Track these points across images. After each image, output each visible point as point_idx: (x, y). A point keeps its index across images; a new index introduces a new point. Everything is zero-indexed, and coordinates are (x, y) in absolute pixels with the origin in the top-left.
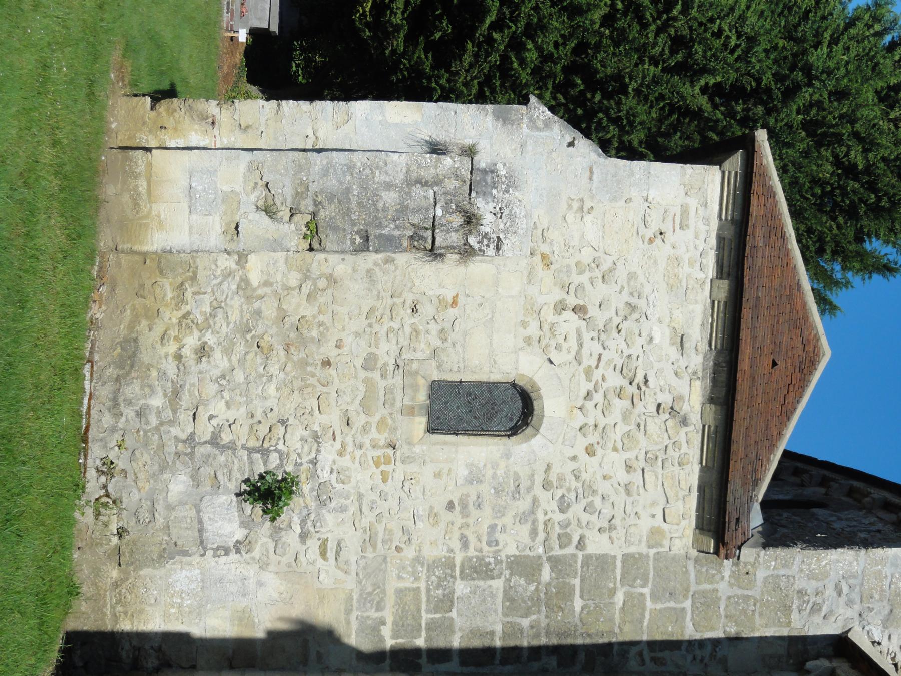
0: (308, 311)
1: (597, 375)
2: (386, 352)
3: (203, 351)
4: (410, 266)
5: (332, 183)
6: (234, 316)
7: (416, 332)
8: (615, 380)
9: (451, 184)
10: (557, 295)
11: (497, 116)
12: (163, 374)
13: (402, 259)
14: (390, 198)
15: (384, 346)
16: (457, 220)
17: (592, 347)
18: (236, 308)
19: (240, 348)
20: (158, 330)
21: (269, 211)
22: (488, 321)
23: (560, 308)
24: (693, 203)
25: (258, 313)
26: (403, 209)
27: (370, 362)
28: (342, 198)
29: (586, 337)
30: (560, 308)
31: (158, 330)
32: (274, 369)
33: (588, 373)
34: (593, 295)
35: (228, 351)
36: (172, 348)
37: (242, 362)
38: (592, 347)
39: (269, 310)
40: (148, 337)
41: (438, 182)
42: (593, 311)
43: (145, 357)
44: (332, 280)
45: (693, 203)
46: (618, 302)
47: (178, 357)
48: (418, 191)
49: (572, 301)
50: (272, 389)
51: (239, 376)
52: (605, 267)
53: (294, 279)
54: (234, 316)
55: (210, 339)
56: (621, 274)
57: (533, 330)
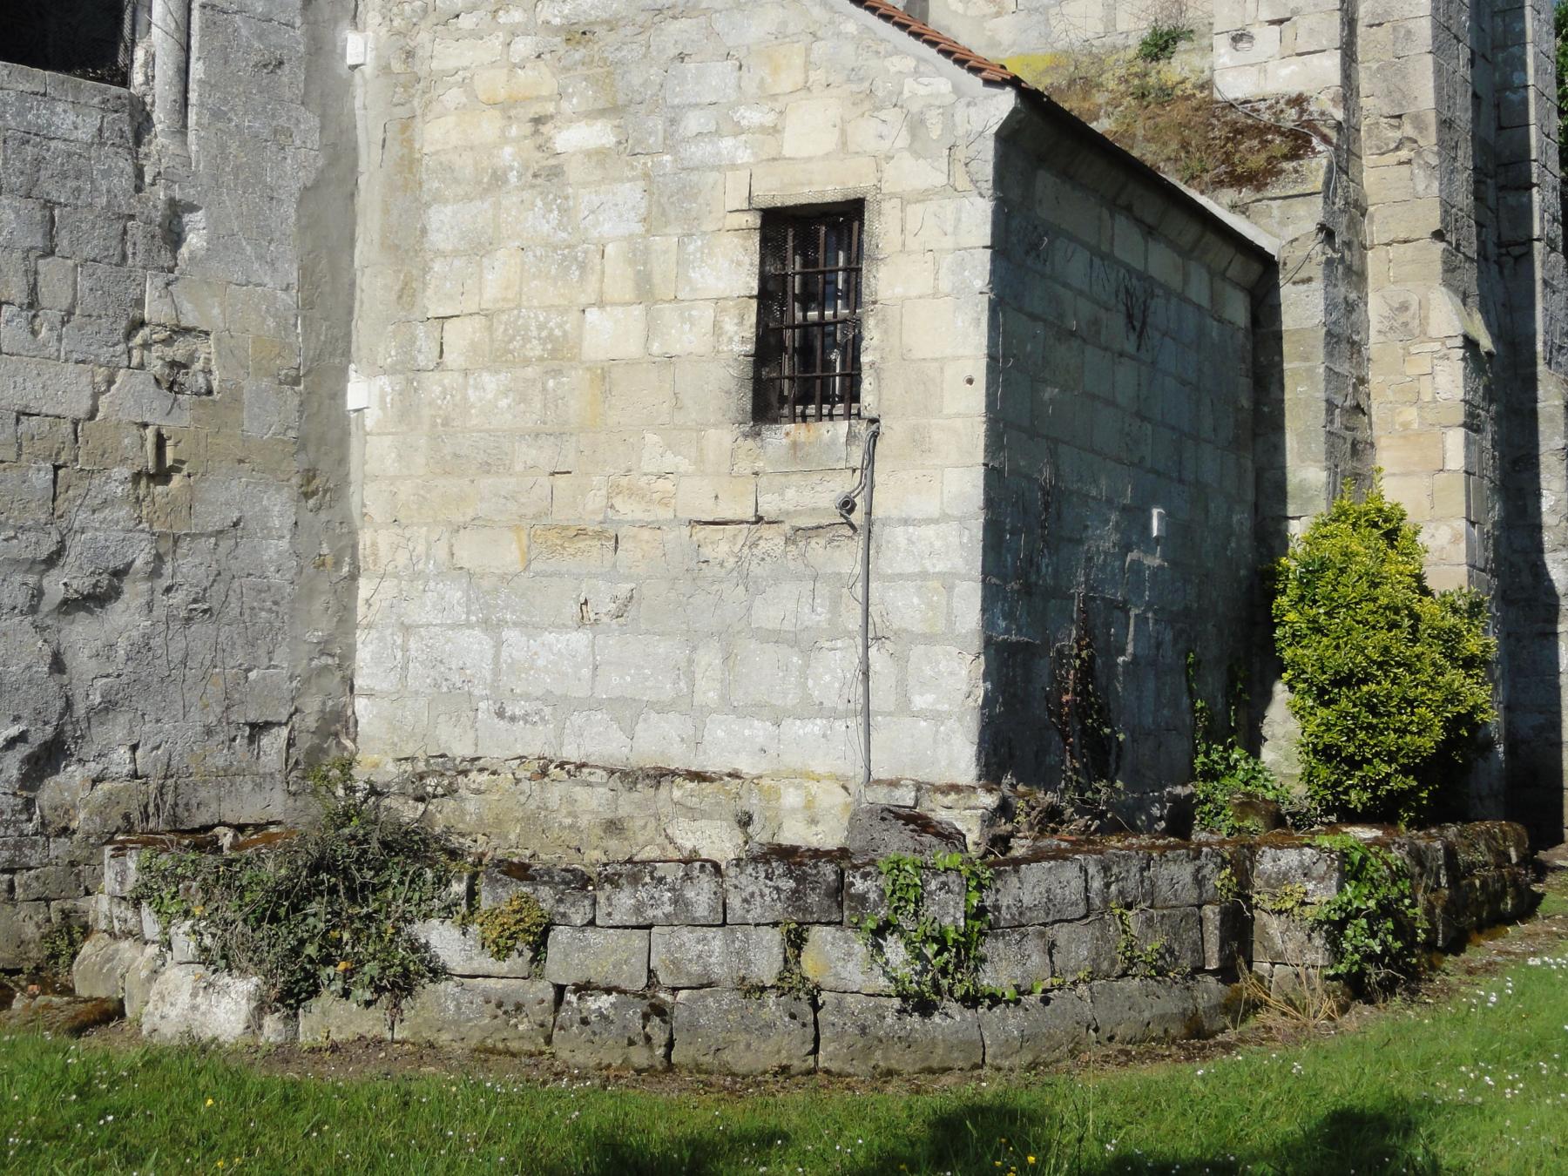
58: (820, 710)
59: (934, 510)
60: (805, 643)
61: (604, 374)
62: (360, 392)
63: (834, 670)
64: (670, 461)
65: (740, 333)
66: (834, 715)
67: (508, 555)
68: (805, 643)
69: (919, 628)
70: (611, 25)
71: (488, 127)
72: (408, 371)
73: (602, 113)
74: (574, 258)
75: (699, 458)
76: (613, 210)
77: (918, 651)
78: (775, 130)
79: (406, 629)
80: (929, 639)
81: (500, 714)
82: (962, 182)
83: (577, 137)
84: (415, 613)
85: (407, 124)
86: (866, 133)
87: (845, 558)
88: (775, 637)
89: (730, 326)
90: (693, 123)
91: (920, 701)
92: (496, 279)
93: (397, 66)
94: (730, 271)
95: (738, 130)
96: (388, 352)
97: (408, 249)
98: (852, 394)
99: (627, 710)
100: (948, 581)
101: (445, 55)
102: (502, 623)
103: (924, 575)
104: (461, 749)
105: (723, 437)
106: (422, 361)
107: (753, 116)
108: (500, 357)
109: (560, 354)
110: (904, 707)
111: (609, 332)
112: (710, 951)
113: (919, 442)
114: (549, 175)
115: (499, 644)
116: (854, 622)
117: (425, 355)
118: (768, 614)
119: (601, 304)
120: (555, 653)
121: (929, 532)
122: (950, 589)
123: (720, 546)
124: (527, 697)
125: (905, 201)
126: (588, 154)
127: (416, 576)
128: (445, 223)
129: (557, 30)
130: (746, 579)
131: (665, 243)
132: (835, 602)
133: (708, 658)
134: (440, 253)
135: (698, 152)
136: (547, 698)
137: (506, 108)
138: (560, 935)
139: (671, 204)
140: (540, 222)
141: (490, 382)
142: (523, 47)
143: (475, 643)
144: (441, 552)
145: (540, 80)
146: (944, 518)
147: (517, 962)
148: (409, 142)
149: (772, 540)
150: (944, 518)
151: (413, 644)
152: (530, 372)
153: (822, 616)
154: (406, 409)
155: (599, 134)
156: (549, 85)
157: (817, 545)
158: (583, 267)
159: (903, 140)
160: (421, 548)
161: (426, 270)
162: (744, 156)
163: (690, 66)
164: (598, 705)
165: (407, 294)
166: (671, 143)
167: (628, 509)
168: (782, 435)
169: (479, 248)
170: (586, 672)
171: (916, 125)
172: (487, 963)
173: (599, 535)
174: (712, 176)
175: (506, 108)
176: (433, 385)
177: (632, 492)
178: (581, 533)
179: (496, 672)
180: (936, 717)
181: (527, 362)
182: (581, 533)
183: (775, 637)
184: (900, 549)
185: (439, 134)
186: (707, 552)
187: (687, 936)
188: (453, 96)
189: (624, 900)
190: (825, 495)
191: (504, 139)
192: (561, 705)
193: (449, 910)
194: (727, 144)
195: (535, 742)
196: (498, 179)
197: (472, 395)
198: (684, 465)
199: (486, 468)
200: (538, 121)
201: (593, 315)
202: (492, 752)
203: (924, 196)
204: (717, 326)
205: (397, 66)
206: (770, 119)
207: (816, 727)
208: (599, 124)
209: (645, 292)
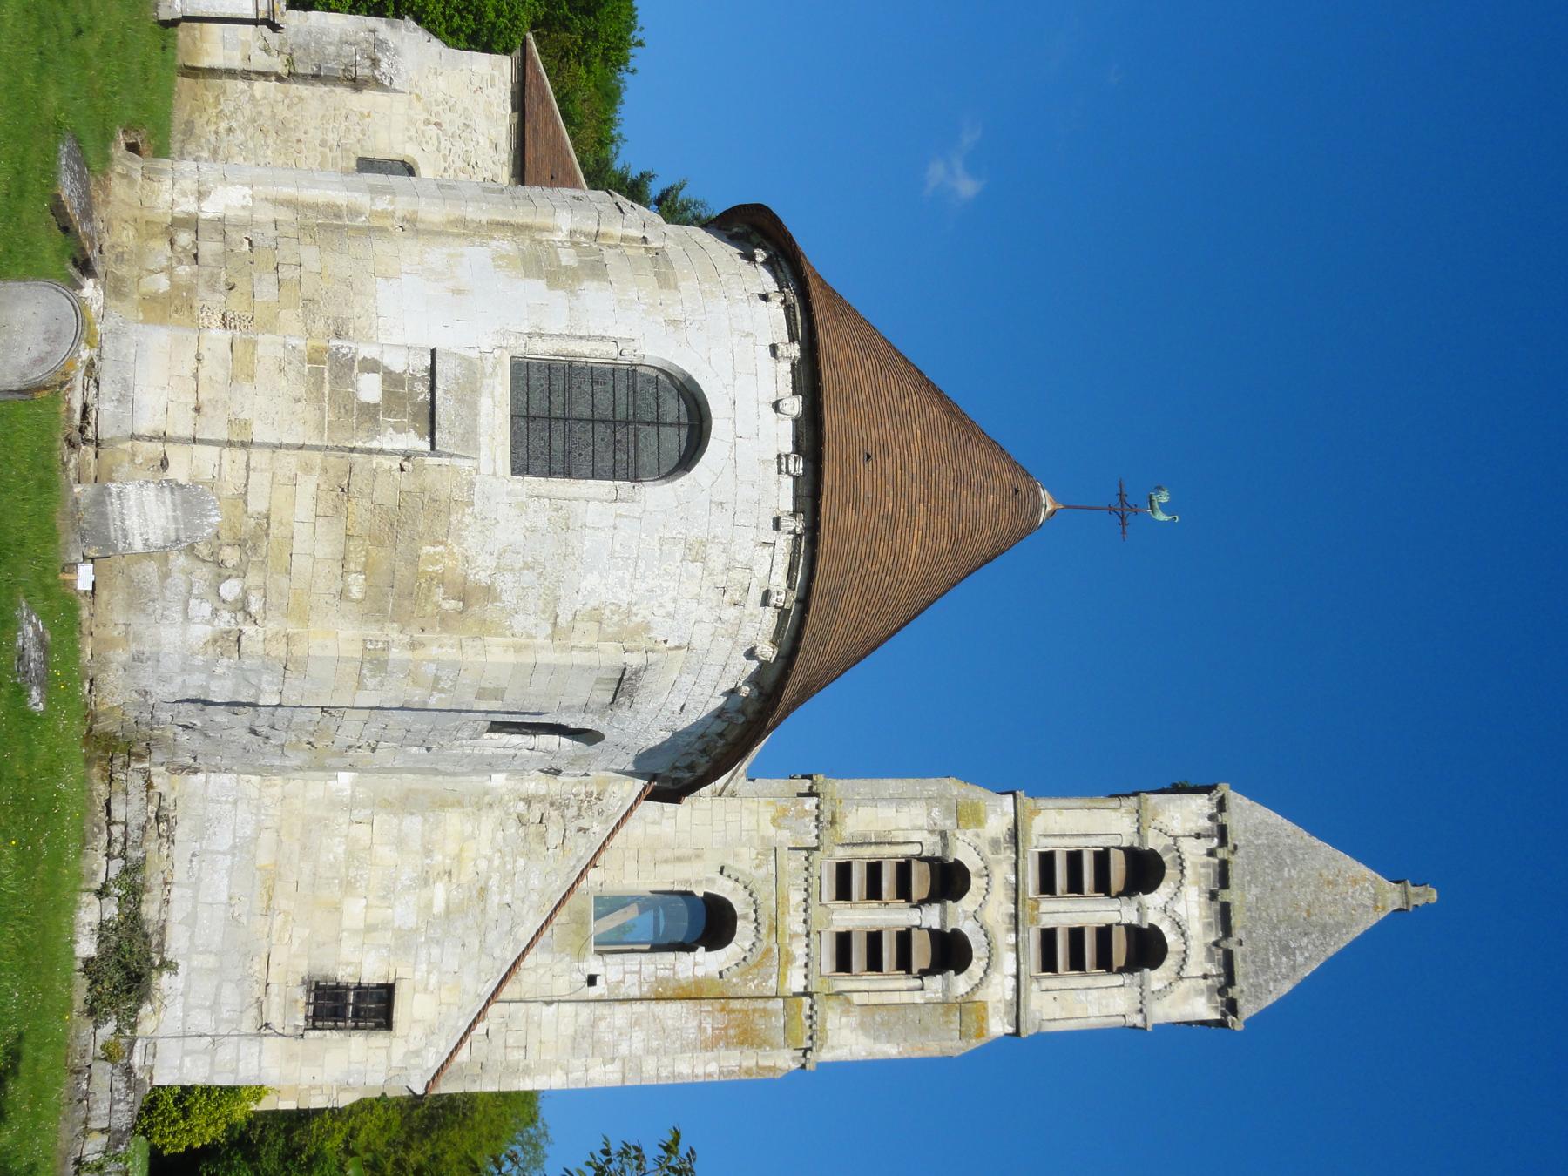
0: (288, 114)
1: (450, 159)
2: (332, 138)
3: (230, 130)
4: (342, 93)
5: (300, 40)
6: (247, 113)
7: (348, 129)
8: (460, 164)
9: (364, 45)
10: (425, 116)
11: (388, 24)
12: (208, 141)
13: (339, 90)
14: (331, 49)
15: (331, 136)
16: (368, 63)
17: (445, 145)
18: (248, 110)
19: (251, 130)
20: (205, 118)
21: (266, 50)
22: (385, 122)
23: (427, 122)
24: (497, 74)
25: (260, 113)
26: (339, 55)
27: (323, 143)
28: (306, 47)
29: (442, 139)
30: (427, 122)
31: (205, 118)
32: (270, 141)
33: (445, 158)
34: (446, 118)
35: (244, 131)
36: (213, 128)
37: (252, 137)
38: (445, 145)
39: (267, 112)
40: (200, 122)
41: (356, 43)
42: (445, 126)
43: (197, 131)
44: (301, 98)
45: (497, 74)
46: (459, 122)
47: (216, 133)
48: (346, 47)
49: (433, 120)
50: (269, 152)
51: (251, 145)
52: (451, 102)
53: (280, 97)
54: (247, 113)
55: (234, 124)
56: (459, 107)
57: (413, 133)
58: (186, 1015)
59: (264, 1064)
60: (214, 1008)
61: (337, 908)
62: (345, 778)
63: (202, 1021)
64: (296, 942)
65: (345, 975)
66: (184, 1022)
67: (264, 859)
68: (214, 1008)
69: (217, 1058)
70: (483, 911)
71: (452, 848)
72: (351, 805)
73: (448, 907)
74: (388, 893)
75: (297, 956)
76: (404, 913)
77: (208, 1058)
78: (426, 989)
79: (235, 803)
80: (212, 1063)
81: (193, 855)
82: (392, 1073)
83: (439, 894)
84: (242, 807)
85: (460, 804)
86: (418, 1031)
87: (248, 1026)
88: (218, 994)
89: (349, 970)
90: (435, 951)
91: (187, 1060)
92: (385, 853)
93: (487, 798)
94: (372, 975)
95: (429, 972)
96: (361, 794)
97: (406, 804)
98: (314, 1028)
99: (191, 921)
100: (235, 1071)
101: (489, 821)
102: (234, 855)
103: (238, 1061)
104: (179, 834)
105: (303, 968)
106: (355, 812)
107: (433, 979)
108: (351, 855)
109: (348, 886)
110: (186, 1053)
111: (355, 911)
112: (101, 1109)
113: (292, 1057)
114: (425, 880)
115: (224, 853)
116: (222, 1031)
117: (359, 814)
118: (228, 991)
119: (367, 907)
120: (218, 885)
121: (255, 1062)
122: (232, 1072)
123: (258, 966)
124: (200, 869)
125: (388, 1048)
126: (431, 900)
127: (258, 808)
128: (413, 825)
129: (486, 883)
130: (244, 978)
131: (388, 938)
132: (230, 1021)
133: (211, 961)
134: (401, 822)
135: (423, 954)
136: (199, 879)
137: (458, 858)
138: (109, 1066)
139: (405, 942)
140: (407, 875)
141: (340, 850)
142: (483, 865)
143: (224, 841)
144: (268, 823)
145: (466, 875)
146: (260, 1069)
147: (100, 1053)
148: (452, 805)
149: (258, 991)
150: (260, 1069)
151: (228, 806)
152: (343, 870)
153: (225, 1015)
154: (334, 804)
155: (439, 907)
156: (464, 880)
157: (254, 1012)
158: (384, 897)
159: (412, 1048)
160: (271, 812)
161: (395, 815)
162: (418, 975)
163: (459, 950)
164: (195, 907)
165: (386, 805)
166: (431, 941)
167: (278, 921)
168: (301, 995)
169: (400, 843)
170: (209, 900)
171: (417, 1053)
172: (100, 1043)
173: (268, 907)
174: (412, 961)
175: (458, 858)
176: (343, 819)
177: (285, 922)
178: (270, 898)
179: (212, 852)
180: (180, 1068)
181: (347, 869)
182: (270, 898)
183: (219, 988)
184: (250, 1049)
185: (454, 821)
186: (256, 959)
187: (107, 1104)
188: (468, 828)
189: (121, 1085)
190: (275, 1018)
191: (444, 857)
192: (196, 886)
193: (119, 1030)
194: (424, 967)
195: (180, 875)
196: (428, 853)
197: (336, 840)
198: (294, 948)
199: (303, 848)
200: (450, 873)
201: (363, 902)
202: (176, 850)
203: (389, 1058)
204: (348, 964)
205: (487, 798)
206: (431, 987)
207: (180, 1014)
208: (443, 905)
209: (370, 929)
